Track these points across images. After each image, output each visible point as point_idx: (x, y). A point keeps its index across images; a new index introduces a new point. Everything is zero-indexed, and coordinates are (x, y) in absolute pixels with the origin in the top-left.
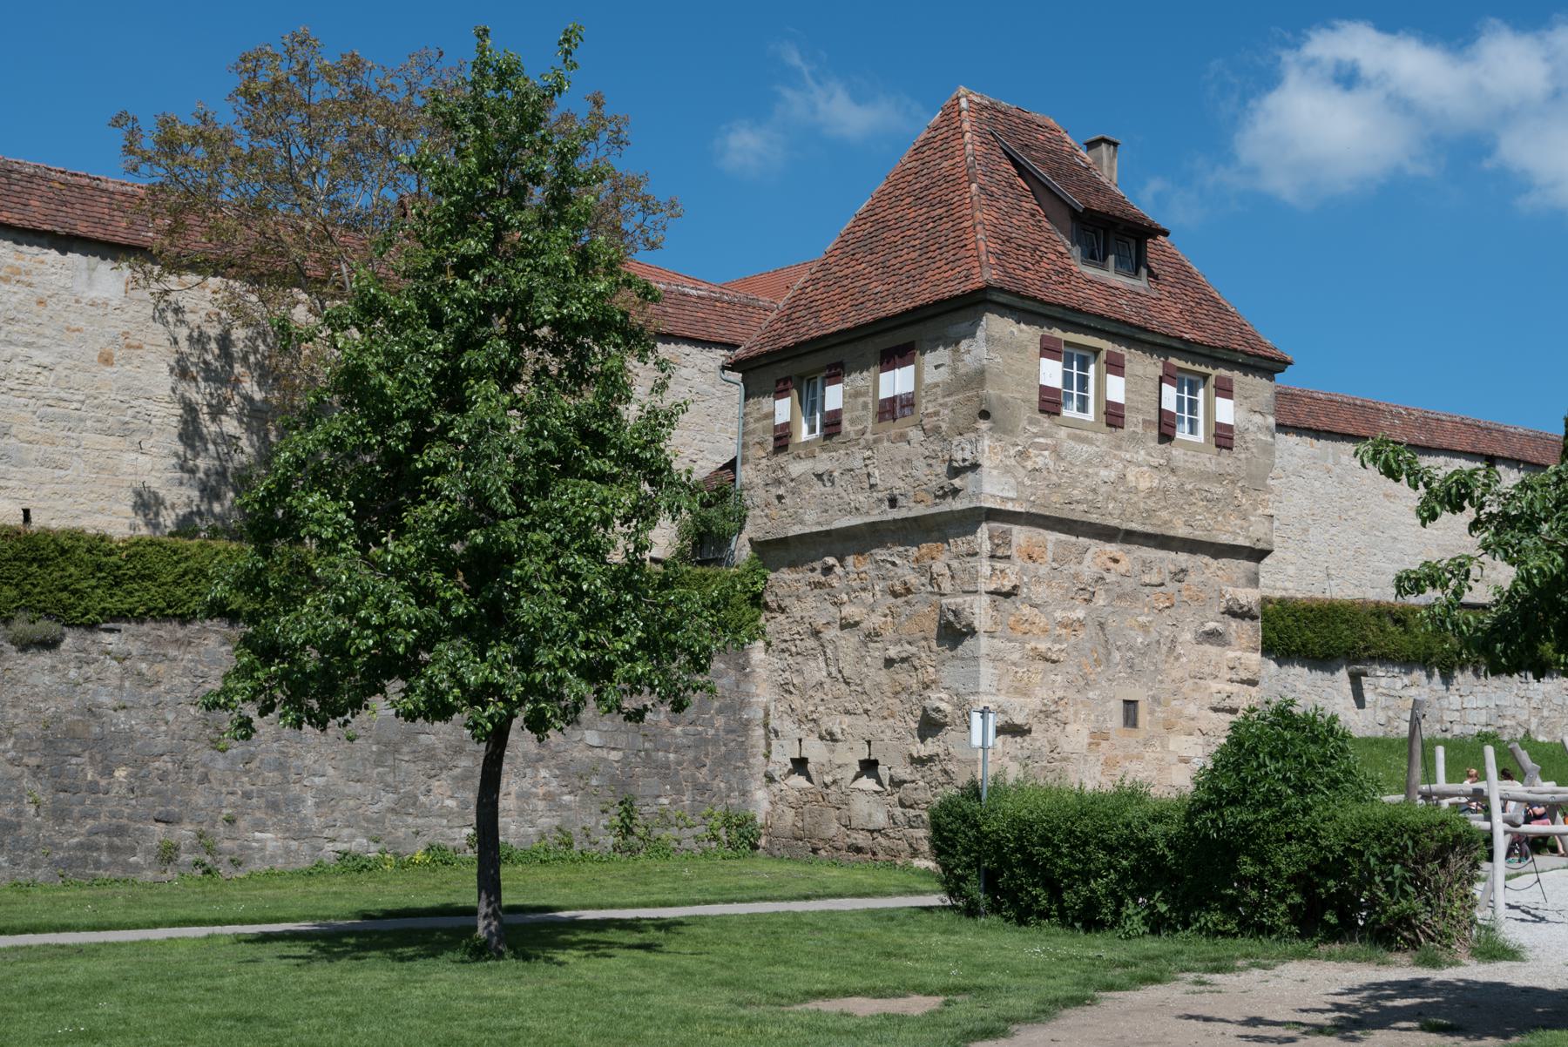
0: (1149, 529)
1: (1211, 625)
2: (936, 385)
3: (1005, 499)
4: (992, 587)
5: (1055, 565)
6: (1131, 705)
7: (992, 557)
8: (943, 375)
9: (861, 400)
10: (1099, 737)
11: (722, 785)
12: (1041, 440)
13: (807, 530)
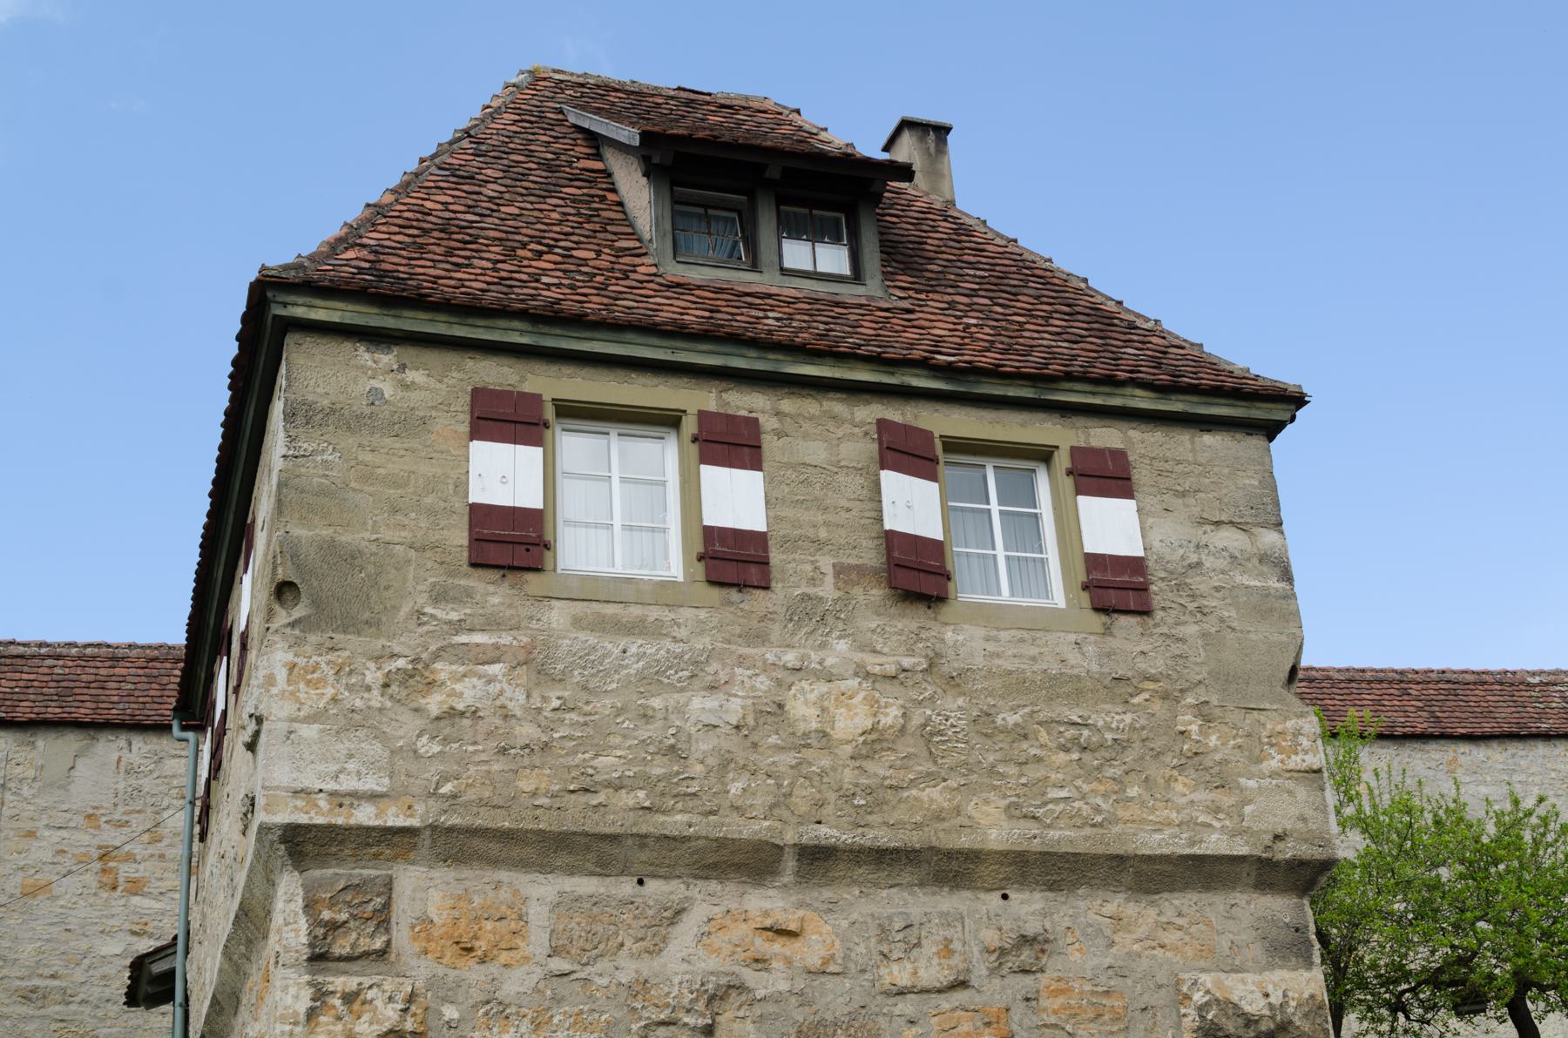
3: (339, 799)
7: (319, 958)
12: (478, 638)
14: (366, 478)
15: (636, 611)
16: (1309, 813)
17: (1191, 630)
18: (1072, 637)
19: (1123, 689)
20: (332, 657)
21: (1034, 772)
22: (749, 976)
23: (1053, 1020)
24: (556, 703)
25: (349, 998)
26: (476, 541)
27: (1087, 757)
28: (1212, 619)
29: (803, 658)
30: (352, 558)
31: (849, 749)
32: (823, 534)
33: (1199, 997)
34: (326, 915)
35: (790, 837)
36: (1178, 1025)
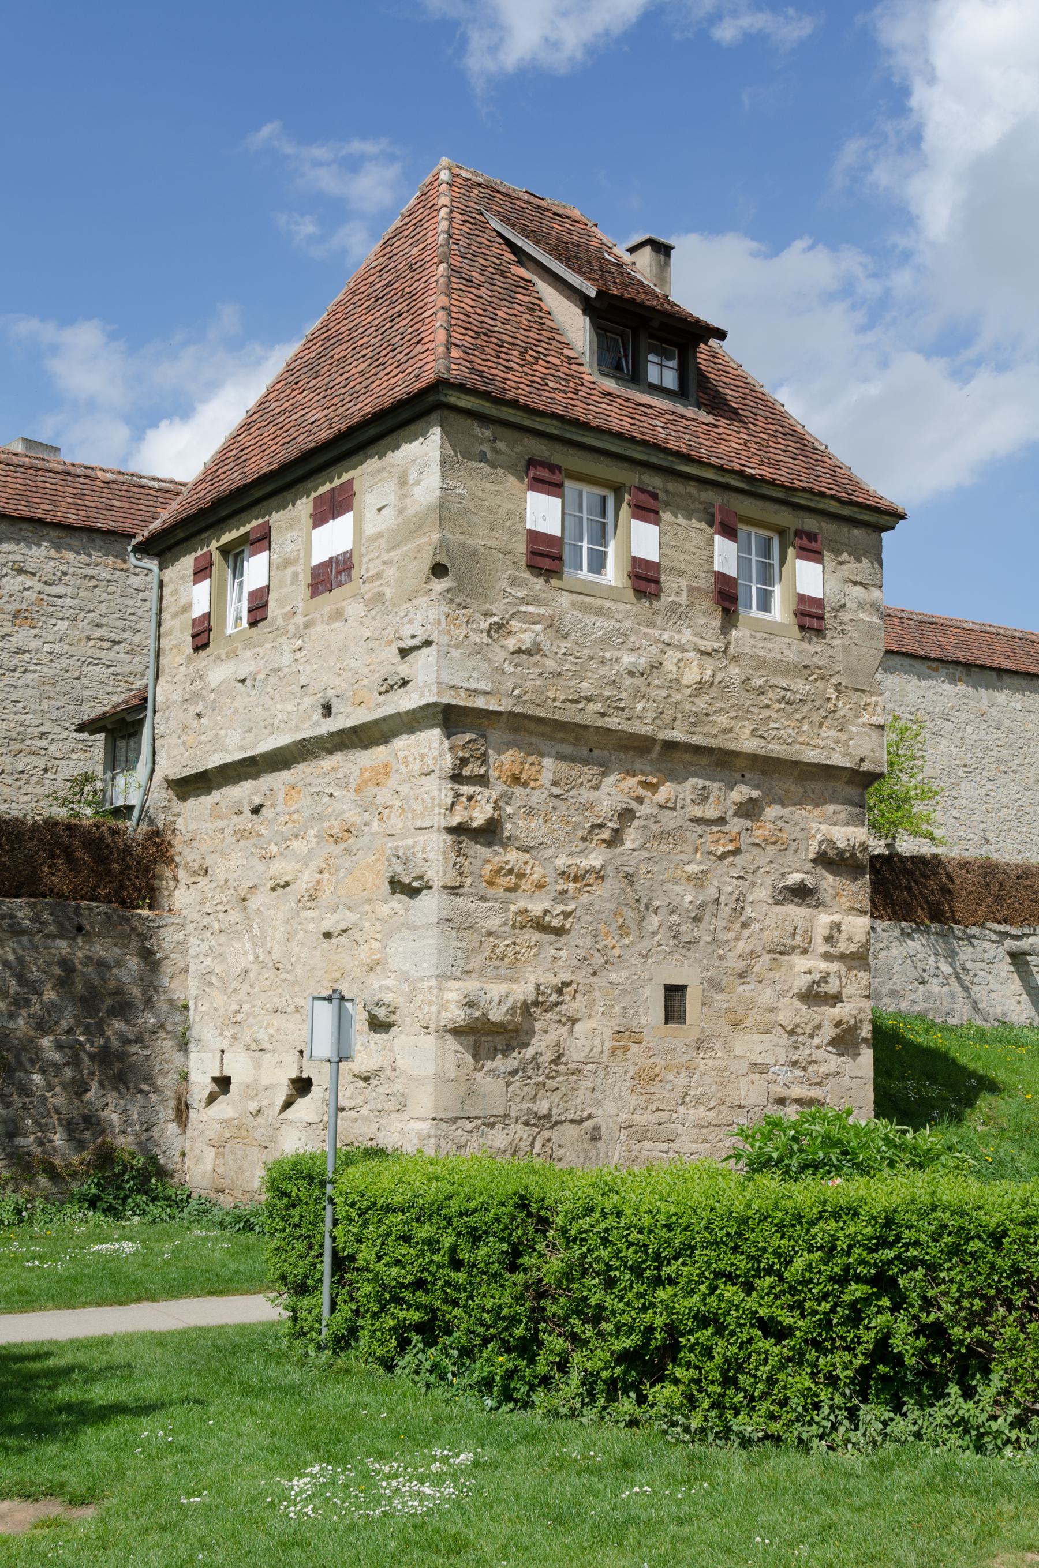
0: (699, 740)
1: (795, 878)
2: (379, 535)
3: (472, 692)
4: (455, 820)
5: (556, 791)
6: (674, 993)
7: (456, 778)
8: (387, 520)
9: (290, 570)
10: (626, 1037)
11: (115, 1117)
12: (530, 609)
13: (228, 759)
14: (480, 506)
15: (600, 602)
16: (876, 747)
17: (837, 642)
18: (787, 640)
19: (807, 672)
20: (464, 611)
21: (767, 713)
22: (634, 805)
23: (757, 841)
24: (564, 650)
25: (470, 798)
26: (534, 553)
27: (788, 707)
28: (847, 637)
29: (671, 638)
30: (471, 554)
31: (688, 691)
32: (683, 567)
33: (819, 837)
34: (460, 754)
35: (662, 735)
36: (807, 850)
